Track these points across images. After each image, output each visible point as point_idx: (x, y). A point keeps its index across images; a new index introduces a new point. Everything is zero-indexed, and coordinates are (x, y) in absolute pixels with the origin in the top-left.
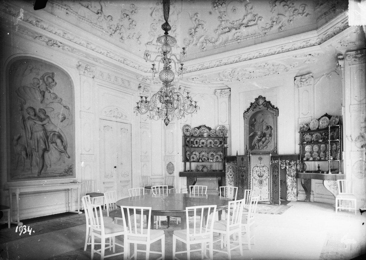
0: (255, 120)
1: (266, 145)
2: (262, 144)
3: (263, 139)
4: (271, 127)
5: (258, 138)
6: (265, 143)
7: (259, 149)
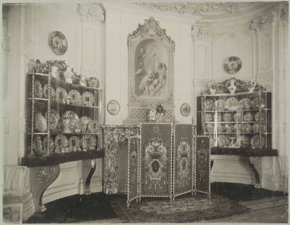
0: (144, 52)
1: (158, 91)
2: (153, 88)
3: (155, 81)
4: (165, 66)
5: (148, 79)
6: (157, 88)
7: (149, 94)
